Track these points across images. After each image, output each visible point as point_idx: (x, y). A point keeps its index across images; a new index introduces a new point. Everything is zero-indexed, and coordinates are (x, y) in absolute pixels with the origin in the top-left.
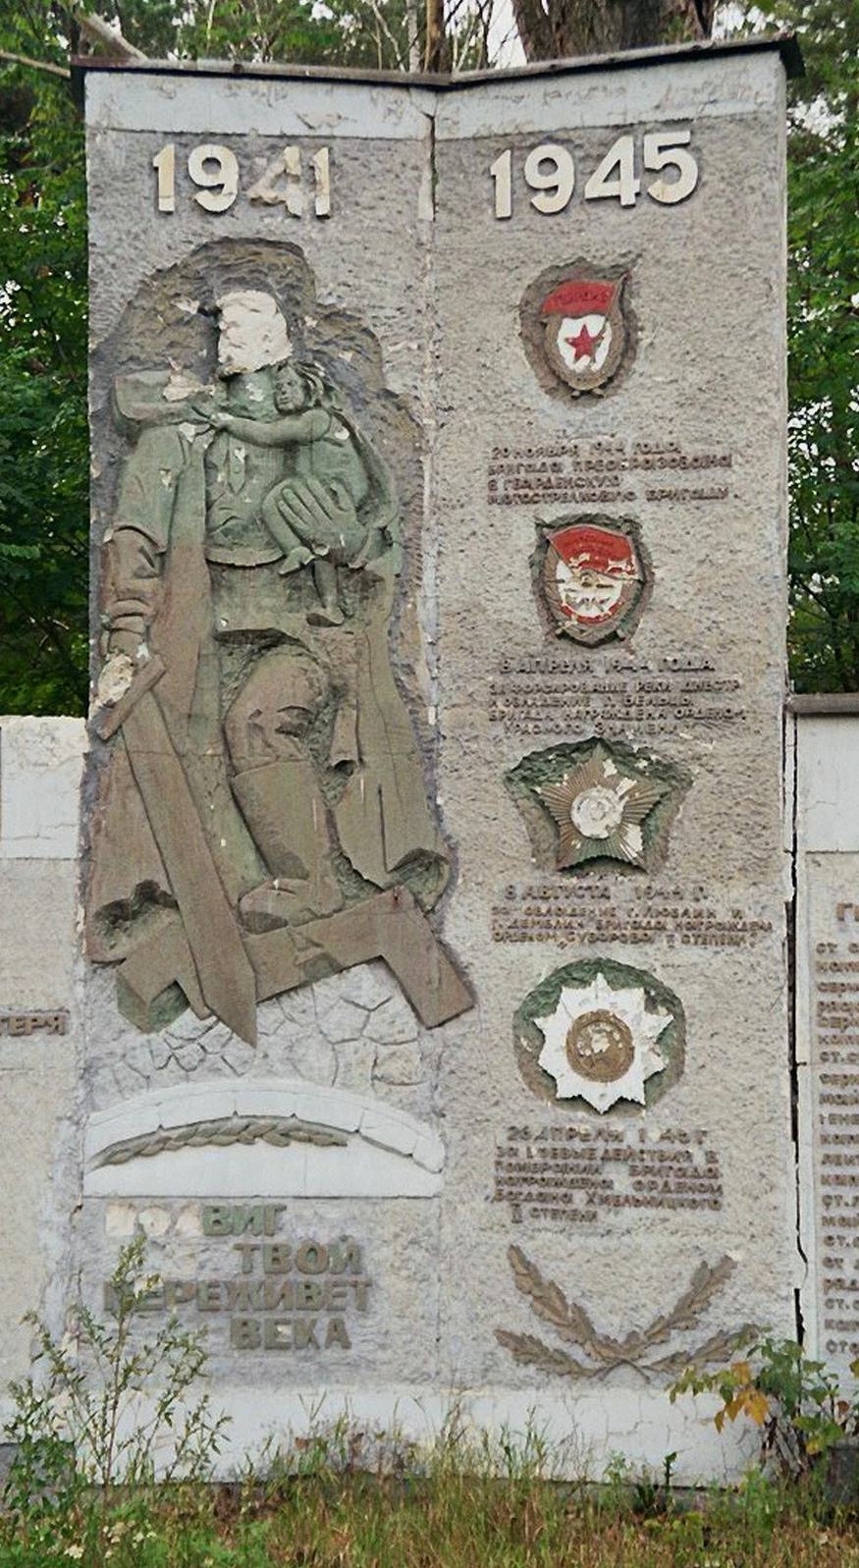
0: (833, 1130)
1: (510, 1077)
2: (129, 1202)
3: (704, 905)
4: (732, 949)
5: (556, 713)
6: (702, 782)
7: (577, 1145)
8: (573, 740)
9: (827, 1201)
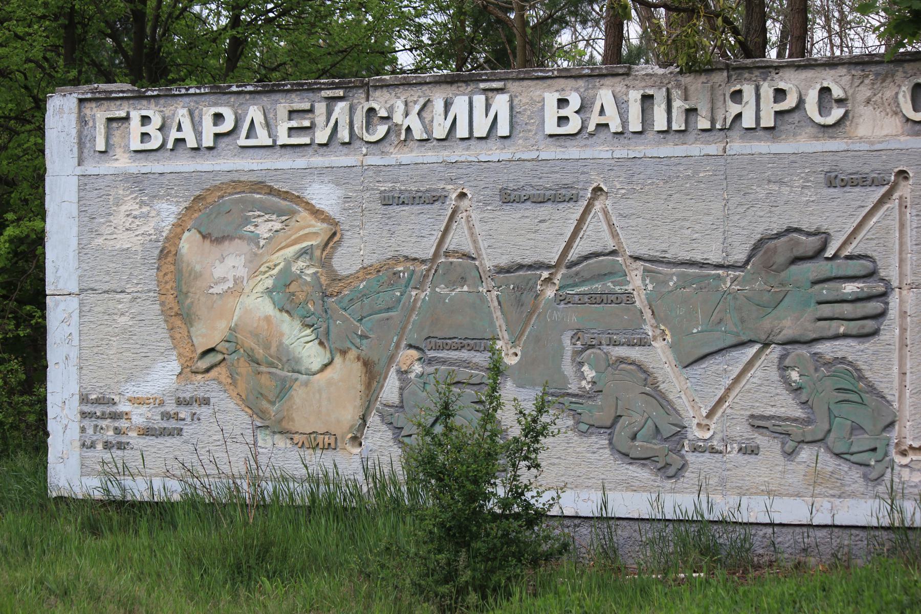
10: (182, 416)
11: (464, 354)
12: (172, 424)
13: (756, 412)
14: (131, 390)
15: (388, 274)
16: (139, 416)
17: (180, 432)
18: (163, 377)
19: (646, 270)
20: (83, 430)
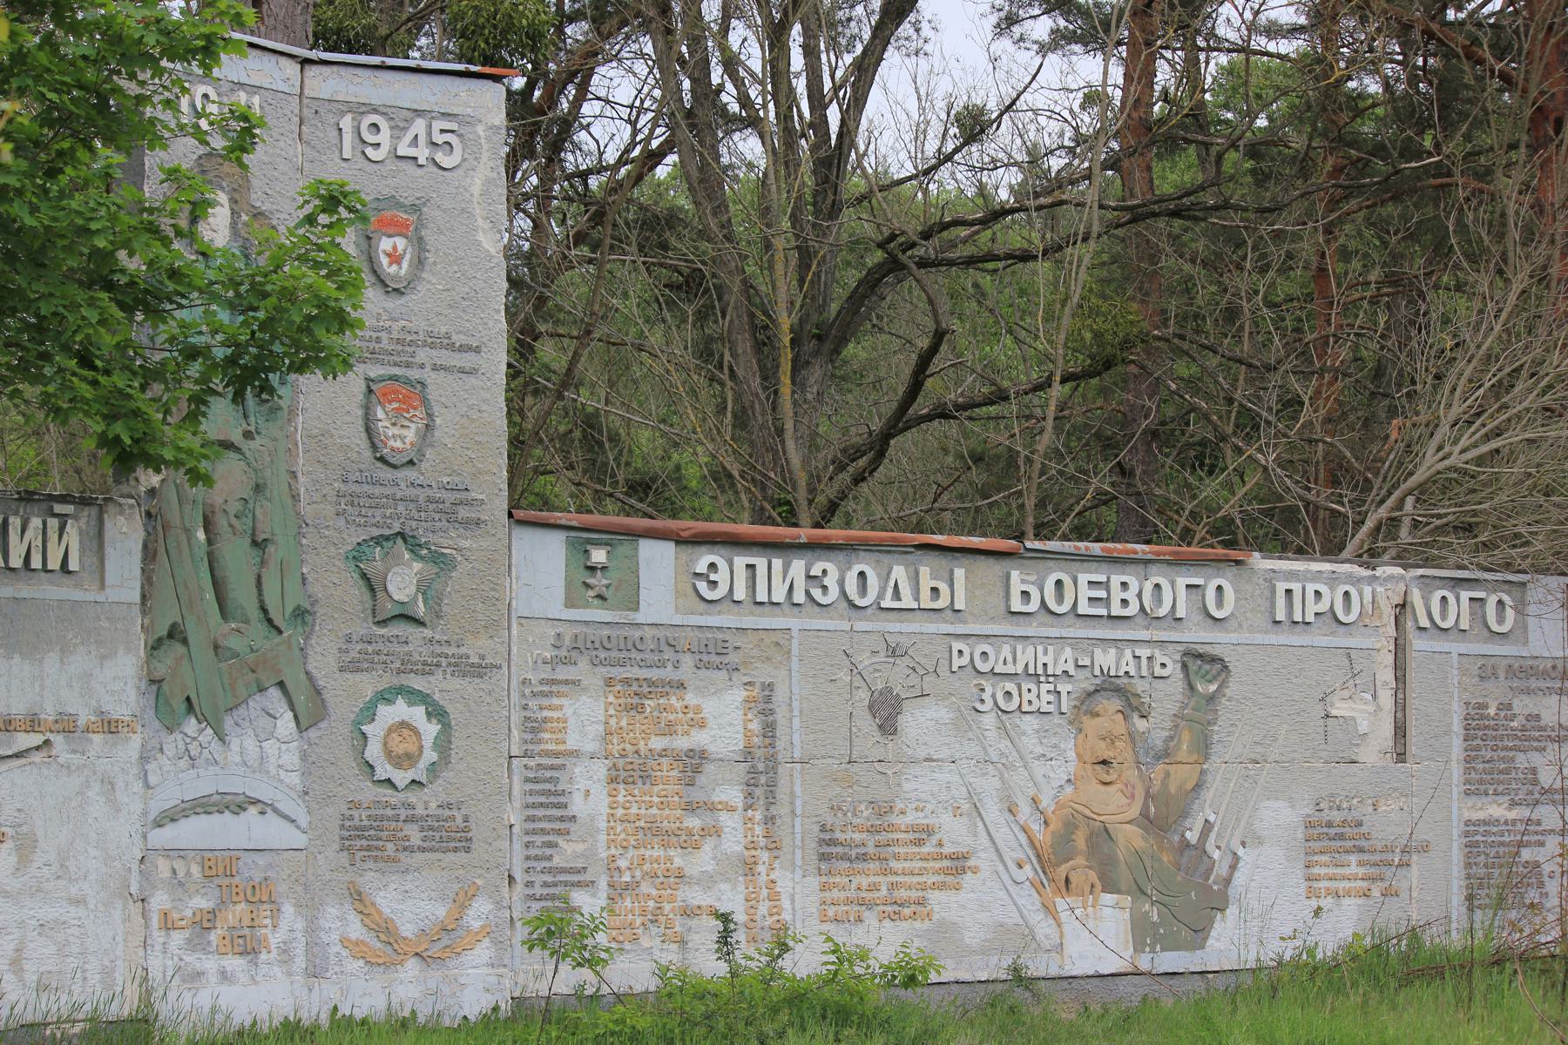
0: (531, 800)
1: (350, 767)
2: (167, 852)
3: (463, 650)
4: (477, 680)
5: (378, 513)
6: (464, 566)
7: (389, 812)
8: (387, 532)
9: (527, 845)
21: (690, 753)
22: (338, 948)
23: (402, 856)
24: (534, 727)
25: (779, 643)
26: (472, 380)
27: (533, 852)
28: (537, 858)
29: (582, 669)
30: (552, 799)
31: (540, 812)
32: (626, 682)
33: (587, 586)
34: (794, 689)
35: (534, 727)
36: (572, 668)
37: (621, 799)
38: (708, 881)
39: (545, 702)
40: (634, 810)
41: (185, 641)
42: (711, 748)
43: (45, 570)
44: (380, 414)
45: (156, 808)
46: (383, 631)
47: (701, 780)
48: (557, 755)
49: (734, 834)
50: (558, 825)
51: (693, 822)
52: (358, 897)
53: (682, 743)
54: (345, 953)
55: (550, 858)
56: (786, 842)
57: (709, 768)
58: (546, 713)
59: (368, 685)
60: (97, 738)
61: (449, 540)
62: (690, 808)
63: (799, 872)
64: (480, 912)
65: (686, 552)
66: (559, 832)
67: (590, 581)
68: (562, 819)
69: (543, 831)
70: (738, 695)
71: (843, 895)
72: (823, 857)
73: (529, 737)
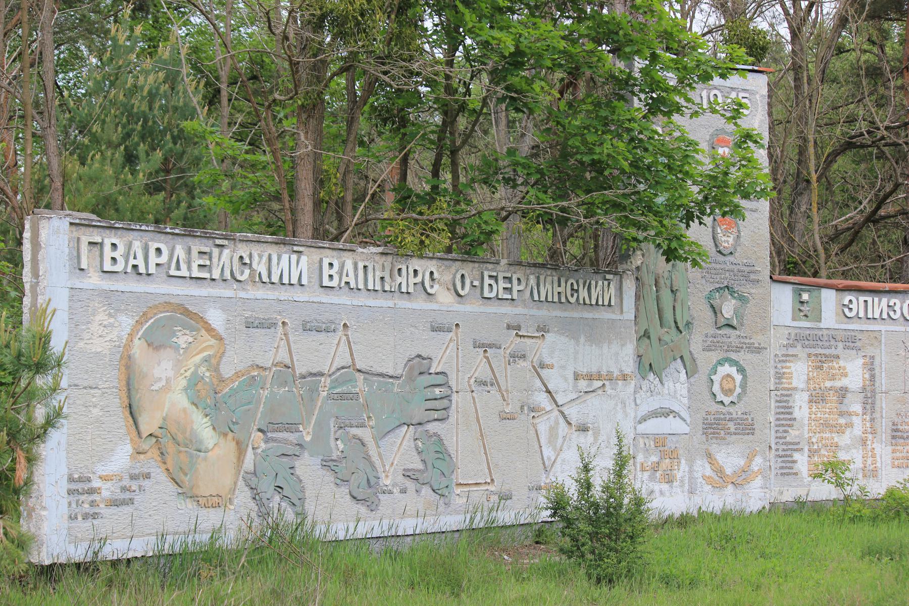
0: (778, 410)
1: (708, 396)
3: (752, 341)
5: (718, 277)
6: (752, 302)
7: (722, 416)
8: (722, 286)
10: (133, 488)
11: (285, 435)
12: (127, 495)
13: (406, 467)
14: (101, 470)
15: (252, 378)
16: (107, 490)
17: (131, 501)
18: (121, 458)
19: (365, 379)
20: (70, 504)
21: (841, 388)
22: (701, 480)
23: (727, 436)
24: (779, 376)
25: (876, 337)
26: (756, 215)
27: (779, 435)
28: (780, 438)
29: (798, 350)
30: (787, 410)
31: (782, 416)
32: (816, 355)
33: (800, 310)
34: (883, 358)
35: (779, 376)
36: (795, 349)
37: (813, 410)
38: (848, 448)
39: (784, 365)
40: (819, 415)
41: (649, 338)
42: (849, 386)
43: (603, 305)
44: (719, 231)
45: (640, 414)
46: (720, 332)
47: (846, 401)
48: (788, 389)
49: (859, 425)
50: (789, 422)
51: (842, 421)
52: (709, 456)
53: (838, 384)
54: (704, 482)
55: (785, 438)
56: (879, 430)
57: (849, 395)
58: (784, 370)
59: (714, 356)
60: (620, 382)
61: (747, 290)
62: (841, 414)
63: (884, 444)
64: (758, 461)
65: (840, 293)
66: (789, 426)
67: (802, 308)
68: (790, 419)
69: (783, 425)
70: (861, 361)
71: (901, 455)
72: (894, 437)
73: (777, 381)
